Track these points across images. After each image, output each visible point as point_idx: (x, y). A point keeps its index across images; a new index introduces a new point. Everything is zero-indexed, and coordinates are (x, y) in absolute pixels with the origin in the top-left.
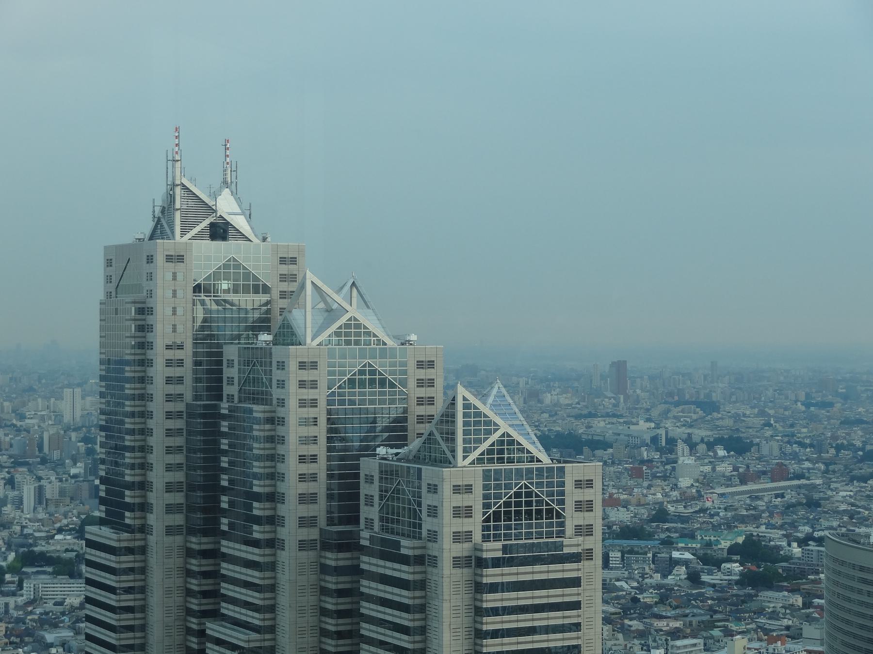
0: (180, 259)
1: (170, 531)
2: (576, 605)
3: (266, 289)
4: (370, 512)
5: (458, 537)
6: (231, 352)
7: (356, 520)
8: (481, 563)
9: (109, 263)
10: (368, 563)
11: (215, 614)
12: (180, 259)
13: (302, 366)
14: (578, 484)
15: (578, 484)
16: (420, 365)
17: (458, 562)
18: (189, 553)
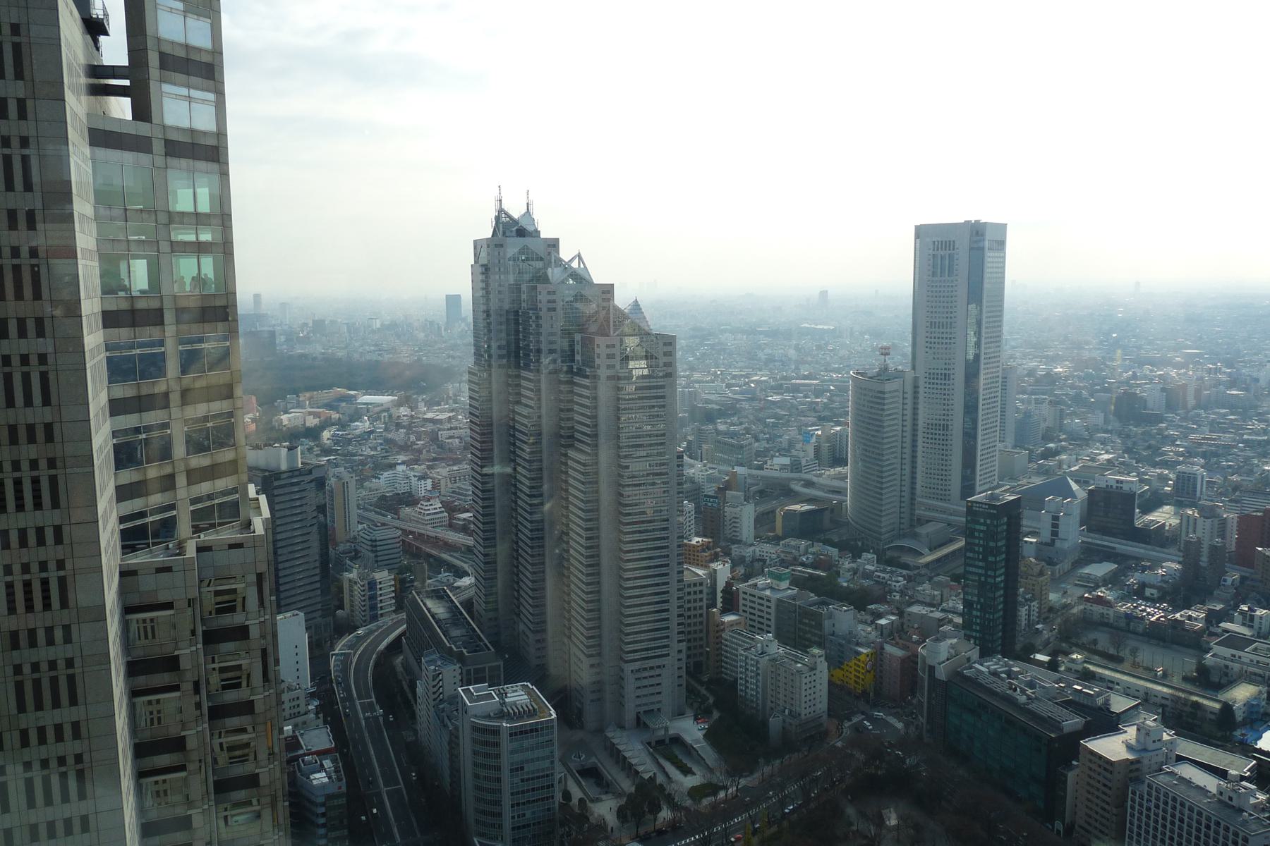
0: (502, 246)
1: (500, 366)
2: (663, 397)
3: (541, 259)
4: (578, 357)
5: (609, 367)
6: (524, 288)
7: (573, 361)
8: (619, 378)
9: (475, 248)
10: (577, 379)
11: (518, 403)
12: (502, 246)
13: (549, 293)
14: (665, 344)
15: (665, 344)
16: (603, 292)
17: (609, 378)
18: (509, 376)
